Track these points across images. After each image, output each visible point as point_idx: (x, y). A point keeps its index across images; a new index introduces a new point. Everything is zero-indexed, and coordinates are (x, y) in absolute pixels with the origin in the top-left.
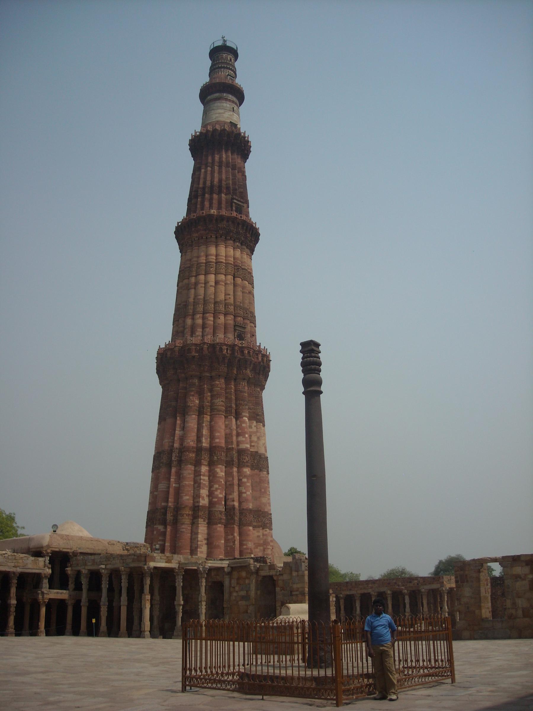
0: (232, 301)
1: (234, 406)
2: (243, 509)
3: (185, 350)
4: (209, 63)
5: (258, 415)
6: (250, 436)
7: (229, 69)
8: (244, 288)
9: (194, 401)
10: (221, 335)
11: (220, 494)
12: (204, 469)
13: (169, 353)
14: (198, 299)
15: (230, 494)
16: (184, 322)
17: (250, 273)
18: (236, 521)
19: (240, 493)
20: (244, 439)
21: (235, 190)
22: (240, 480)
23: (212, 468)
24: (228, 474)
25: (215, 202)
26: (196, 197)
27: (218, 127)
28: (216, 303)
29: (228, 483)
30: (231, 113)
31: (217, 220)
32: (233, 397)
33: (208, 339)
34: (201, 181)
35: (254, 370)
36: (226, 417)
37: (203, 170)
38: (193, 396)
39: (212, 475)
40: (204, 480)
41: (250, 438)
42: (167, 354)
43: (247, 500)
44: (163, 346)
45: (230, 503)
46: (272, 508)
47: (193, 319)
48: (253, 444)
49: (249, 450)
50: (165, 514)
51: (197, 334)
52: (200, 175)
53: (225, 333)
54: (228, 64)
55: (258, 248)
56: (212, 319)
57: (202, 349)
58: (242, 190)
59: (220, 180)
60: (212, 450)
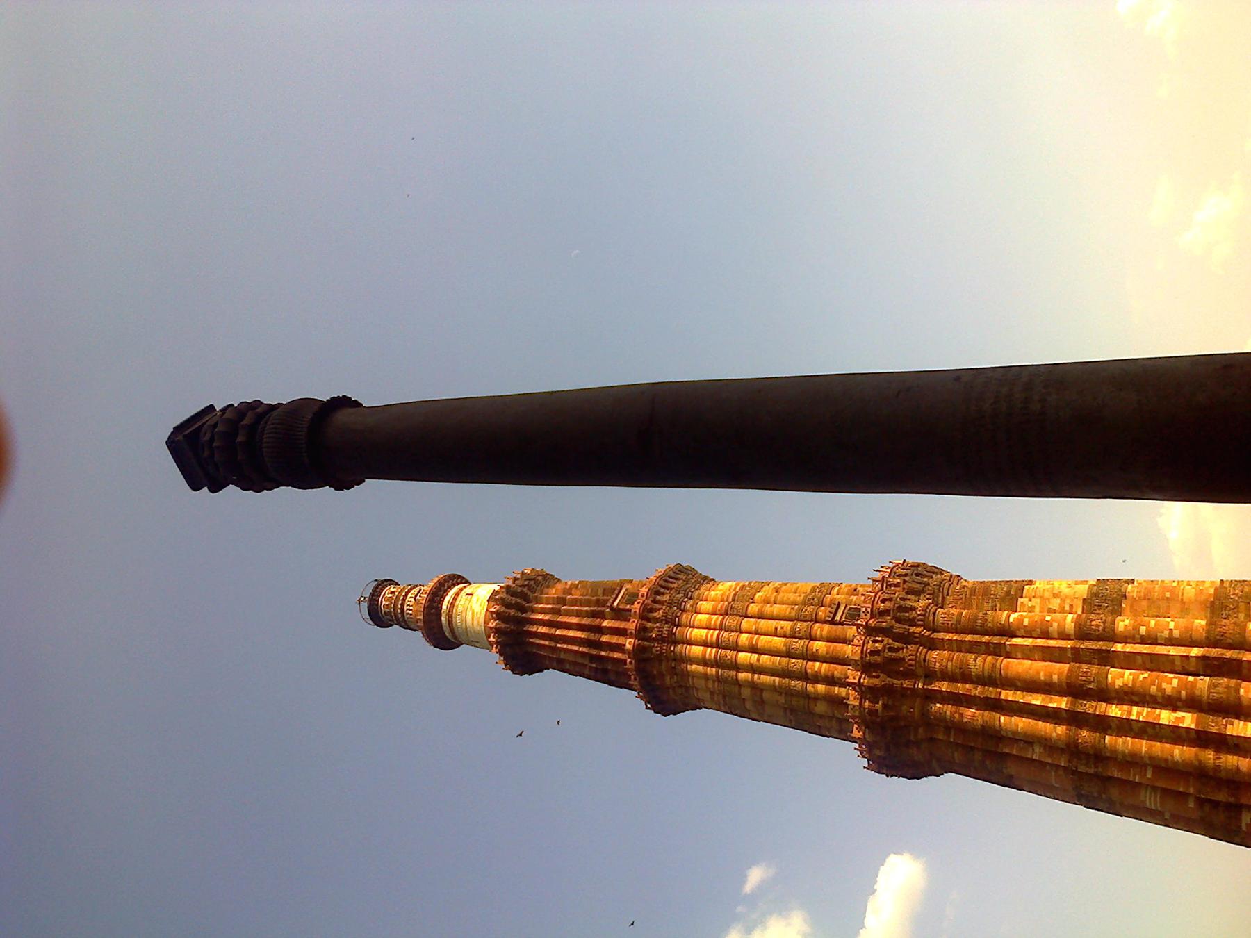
0: (787, 625)
1: (986, 639)
2: (1207, 638)
3: (870, 722)
4: (396, 628)
5: (1008, 593)
6: (1051, 611)
7: (406, 596)
8: (766, 601)
9: (971, 714)
10: (848, 650)
11: (1172, 683)
12: (1115, 711)
13: (878, 752)
14: (780, 686)
15: (1173, 662)
16: (821, 716)
17: (743, 588)
18: (1235, 656)
19: (1171, 642)
20: (1055, 625)
21: (598, 603)
22: (1143, 641)
23: (1113, 695)
24: (1128, 661)
25: (614, 639)
26: (605, 671)
27: (492, 624)
28: (789, 655)
29: (1148, 666)
30: (474, 598)
31: (644, 639)
32: (969, 638)
33: (853, 676)
34: (580, 660)
35: (917, 593)
36: (1008, 656)
37: (562, 656)
38: (961, 715)
39: (1128, 696)
40: (1139, 714)
41: (1055, 611)
42: (879, 757)
43: (1188, 629)
44: (865, 762)
45: (1192, 666)
46: (1208, 579)
47: (816, 698)
48: (1067, 608)
49: (1079, 616)
50: (1216, 804)
51: (844, 694)
52: (570, 662)
53: (844, 642)
54: (398, 597)
55: (702, 570)
56: (817, 664)
57: (869, 688)
58: (600, 591)
59: (580, 627)
60: (1074, 690)
